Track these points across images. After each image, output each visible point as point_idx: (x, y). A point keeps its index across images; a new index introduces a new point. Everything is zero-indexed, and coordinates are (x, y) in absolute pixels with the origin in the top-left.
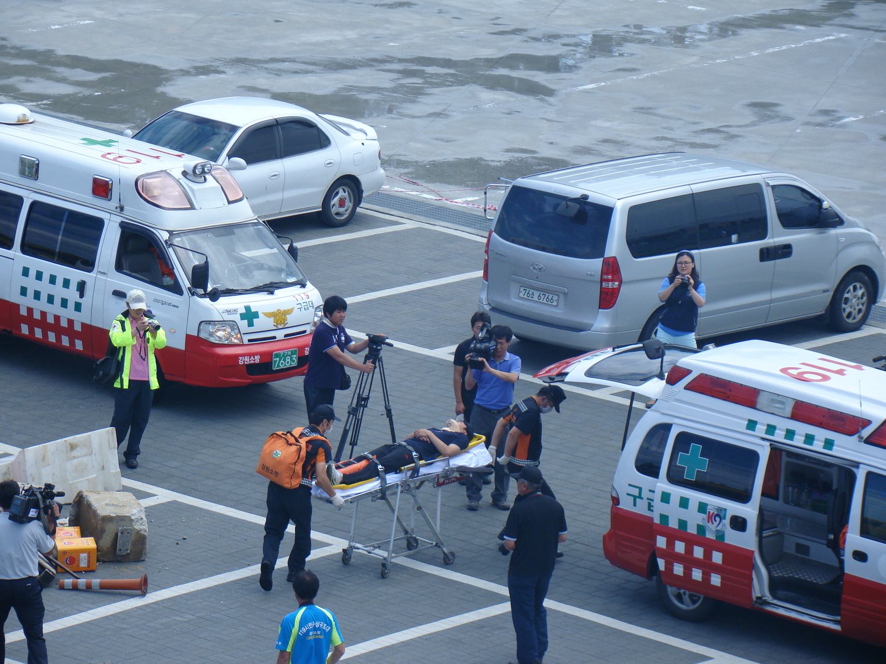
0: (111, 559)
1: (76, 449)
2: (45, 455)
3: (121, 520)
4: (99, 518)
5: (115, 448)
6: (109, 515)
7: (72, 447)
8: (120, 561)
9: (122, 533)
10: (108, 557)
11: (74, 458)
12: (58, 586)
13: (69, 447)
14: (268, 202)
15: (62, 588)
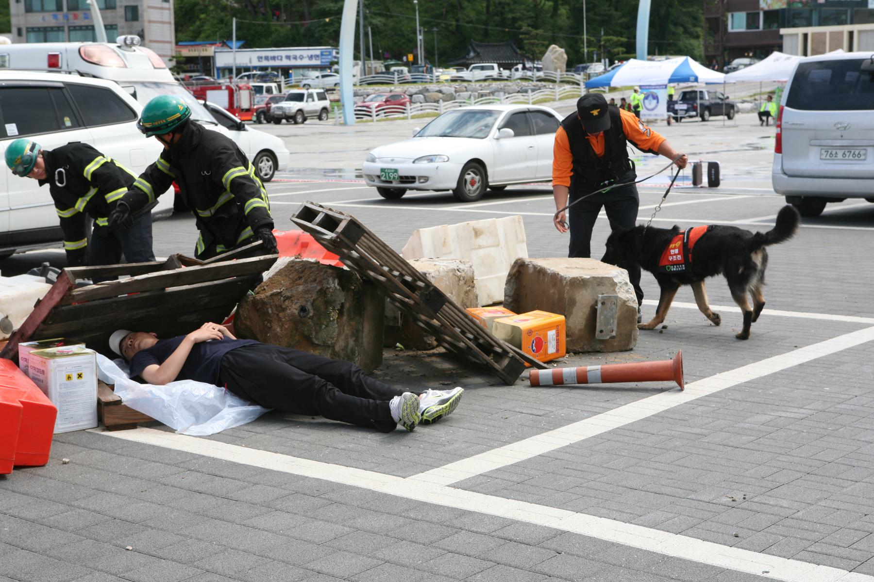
0: (586, 349)
1: (481, 236)
2: (445, 239)
3: (598, 285)
4: (564, 283)
5: (523, 241)
6: (581, 277)
7: (477, 233)
8: (599, 352)
9: (603, 303)
10: (582, 344)
11: (480, 247)
12: (528, 383)
13: (473, 232)
14: (528, 167)
15: (535, 383)
